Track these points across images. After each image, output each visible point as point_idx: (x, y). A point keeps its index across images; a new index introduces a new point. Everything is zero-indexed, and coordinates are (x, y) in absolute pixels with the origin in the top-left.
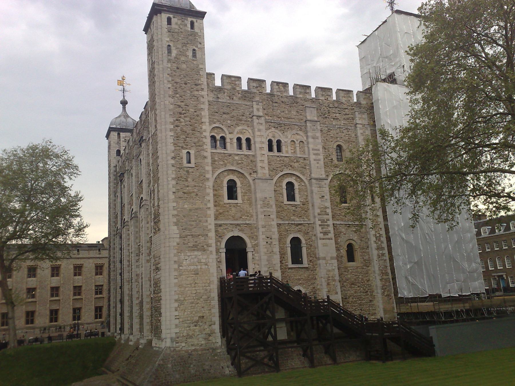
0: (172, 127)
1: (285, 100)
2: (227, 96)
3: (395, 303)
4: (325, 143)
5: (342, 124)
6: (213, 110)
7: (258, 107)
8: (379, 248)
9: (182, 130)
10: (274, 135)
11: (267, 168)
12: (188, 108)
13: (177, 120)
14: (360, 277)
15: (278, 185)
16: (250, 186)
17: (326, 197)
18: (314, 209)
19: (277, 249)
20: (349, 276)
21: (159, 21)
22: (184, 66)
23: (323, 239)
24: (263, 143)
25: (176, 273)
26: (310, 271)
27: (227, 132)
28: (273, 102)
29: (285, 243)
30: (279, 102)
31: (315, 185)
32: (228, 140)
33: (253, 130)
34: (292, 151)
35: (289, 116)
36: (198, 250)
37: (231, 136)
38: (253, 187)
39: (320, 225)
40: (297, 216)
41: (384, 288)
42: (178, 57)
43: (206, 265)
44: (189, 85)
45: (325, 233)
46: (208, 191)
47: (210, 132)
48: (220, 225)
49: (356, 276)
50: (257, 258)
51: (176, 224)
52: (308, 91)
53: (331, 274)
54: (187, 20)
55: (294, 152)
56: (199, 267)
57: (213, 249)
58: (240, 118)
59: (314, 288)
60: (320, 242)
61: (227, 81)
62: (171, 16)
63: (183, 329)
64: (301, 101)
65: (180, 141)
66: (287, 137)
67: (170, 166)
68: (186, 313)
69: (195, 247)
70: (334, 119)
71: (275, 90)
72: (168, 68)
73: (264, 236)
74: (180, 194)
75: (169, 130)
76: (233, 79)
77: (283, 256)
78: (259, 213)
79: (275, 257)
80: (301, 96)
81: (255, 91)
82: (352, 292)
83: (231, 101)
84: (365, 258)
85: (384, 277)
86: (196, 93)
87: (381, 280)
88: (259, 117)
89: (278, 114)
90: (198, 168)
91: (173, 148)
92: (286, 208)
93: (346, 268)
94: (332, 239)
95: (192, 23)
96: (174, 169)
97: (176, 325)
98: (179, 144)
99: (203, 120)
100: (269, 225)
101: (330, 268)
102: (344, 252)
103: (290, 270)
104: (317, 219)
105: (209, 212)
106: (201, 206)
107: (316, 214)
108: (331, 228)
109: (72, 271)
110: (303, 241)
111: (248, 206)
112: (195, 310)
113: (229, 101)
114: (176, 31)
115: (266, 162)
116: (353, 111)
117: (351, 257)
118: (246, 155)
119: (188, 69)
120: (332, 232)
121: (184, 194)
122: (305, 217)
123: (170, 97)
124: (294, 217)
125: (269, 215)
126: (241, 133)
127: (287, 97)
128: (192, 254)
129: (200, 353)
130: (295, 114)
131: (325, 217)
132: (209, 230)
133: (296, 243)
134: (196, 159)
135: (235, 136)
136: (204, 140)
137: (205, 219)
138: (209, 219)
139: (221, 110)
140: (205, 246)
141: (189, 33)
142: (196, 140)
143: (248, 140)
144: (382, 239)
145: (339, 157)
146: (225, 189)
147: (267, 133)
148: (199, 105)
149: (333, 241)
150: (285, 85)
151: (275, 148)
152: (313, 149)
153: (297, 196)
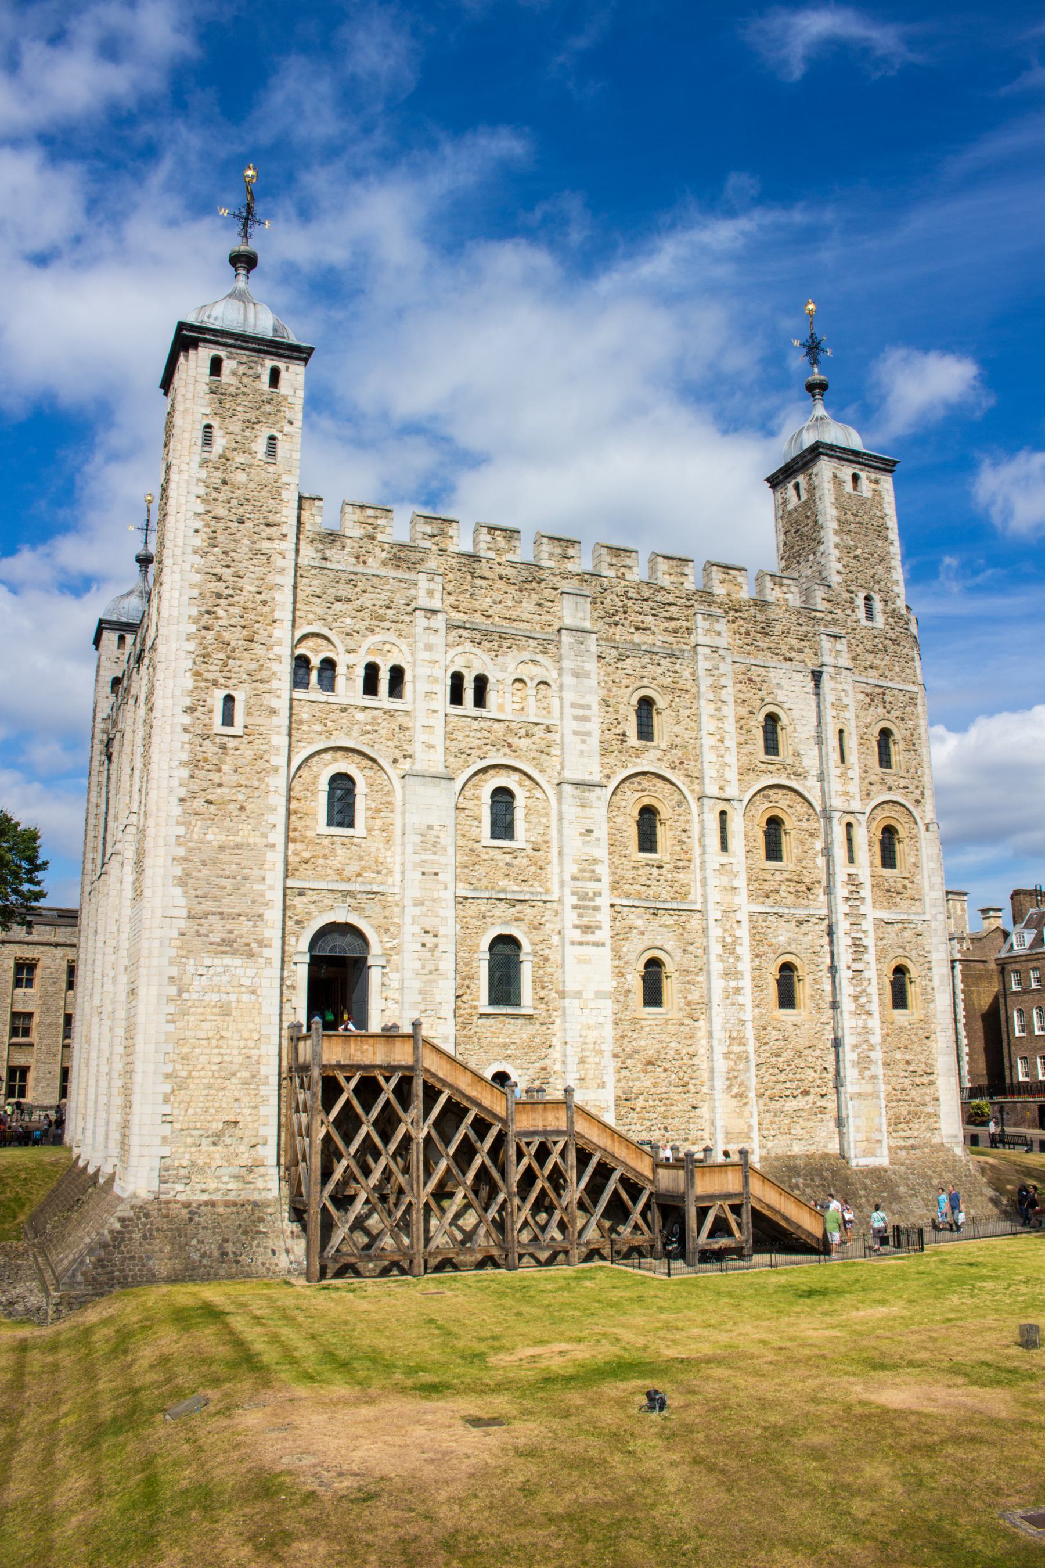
0: (193, 628)
1: (509, 572)
2: (350, 554)
3: (755, 1114)
4: (609, 690)
5: (659, 643)
6: (309, 591)
7: (432, 586)
8: (730, 974)
10: (469, 661)
11: (440, 749)
13: (208, 612)
14: (673, 1045)
15: (468, 793)
17: (596, 834)
18: (561, 864)
19: (447, 964)
20: (643, 1043)
22: (240, 477)
23: (581, 944)
24: (436, 680)
25: (171, 1009)
26: (537, 1026)
29: (474, 950)
32: (341, 669)
34: (517, 706)
35: (513, 614)
37: (351, 659)
39: (575, 907)
41: (732, 1078)
42: (228, 454)
43: (254, 992)
44: (249, 524)
45: (587, 929)
47: (294, 647)
49: (660, 1042)
50: (395, 984)
51: (181, 882)
52: (571, 552)
53: (592, 1036)
54: (262, 365)
55: (522, 709)
56: (233, 997)
57: (274, 953)
58: (381, 611)
59: (544, 1069)
60: (570, 950)
61: (355, 517)
62: (222, 353)
63: (182, 1150)
64: (551, 577)
65: (211, 668)
66: (504, 670)
67: (179, 729)
68: (191, 1111)
69: (227, 946)
72: (199, 480)
73: (417, 929)
74: (198, 804)
75: (184, 636)
76: (370, 512)
77: (466, 983)
78: (409, 866)
79: (442, 983)
81: (428, 544)
82: (648, 1083)
83: (360, 569)
84: (690, 998)
85: (736, 1049)
87: (727, 1055)
89: (485, 606)
91: (189, 682)
92: (486, 857)
93: (635, 1021)
94: (603, 945)
95: (275, 374)
96: (187, 737)
97: (164, 1138)
98: (206, 675)
99: (277, 615)
100: (434, 901)
101: (591, 1022)
102: (635, 982)
103: (482, 1021)
104: (567, 891)
106: (251, 841)
107: (567, 878)
108: (604, 917)
109: (11, 974)
110: (526, 947)
111: (381, 846)
112: (217, 1105)
113: (352, 569)
114: (232, 390)
115: (440, 731)
116: (690, 612)
117: (653, 995)
119: (252, 485)
120: (606, 923)
122: (536, 884)
123: (196, 553)
125: (436, 874)
127: (513, 564)
128: (217, 961)
129: (221, 1210)
131: (591, 886)
133: (505, 952)
136: (275, 666)
137: (261, 872)
138: (269, 875)
139: (331, 591)
140: (254, 945)
141: (264, 398)
143: (397, 674)
144: (739, 950)
145: (645, 729)
147: (450, 655)
148: (270, 577)
149: (606, 952)
150: (511, 534)
151: (469, 695)
152: (573, 705)
153: (520, 826)
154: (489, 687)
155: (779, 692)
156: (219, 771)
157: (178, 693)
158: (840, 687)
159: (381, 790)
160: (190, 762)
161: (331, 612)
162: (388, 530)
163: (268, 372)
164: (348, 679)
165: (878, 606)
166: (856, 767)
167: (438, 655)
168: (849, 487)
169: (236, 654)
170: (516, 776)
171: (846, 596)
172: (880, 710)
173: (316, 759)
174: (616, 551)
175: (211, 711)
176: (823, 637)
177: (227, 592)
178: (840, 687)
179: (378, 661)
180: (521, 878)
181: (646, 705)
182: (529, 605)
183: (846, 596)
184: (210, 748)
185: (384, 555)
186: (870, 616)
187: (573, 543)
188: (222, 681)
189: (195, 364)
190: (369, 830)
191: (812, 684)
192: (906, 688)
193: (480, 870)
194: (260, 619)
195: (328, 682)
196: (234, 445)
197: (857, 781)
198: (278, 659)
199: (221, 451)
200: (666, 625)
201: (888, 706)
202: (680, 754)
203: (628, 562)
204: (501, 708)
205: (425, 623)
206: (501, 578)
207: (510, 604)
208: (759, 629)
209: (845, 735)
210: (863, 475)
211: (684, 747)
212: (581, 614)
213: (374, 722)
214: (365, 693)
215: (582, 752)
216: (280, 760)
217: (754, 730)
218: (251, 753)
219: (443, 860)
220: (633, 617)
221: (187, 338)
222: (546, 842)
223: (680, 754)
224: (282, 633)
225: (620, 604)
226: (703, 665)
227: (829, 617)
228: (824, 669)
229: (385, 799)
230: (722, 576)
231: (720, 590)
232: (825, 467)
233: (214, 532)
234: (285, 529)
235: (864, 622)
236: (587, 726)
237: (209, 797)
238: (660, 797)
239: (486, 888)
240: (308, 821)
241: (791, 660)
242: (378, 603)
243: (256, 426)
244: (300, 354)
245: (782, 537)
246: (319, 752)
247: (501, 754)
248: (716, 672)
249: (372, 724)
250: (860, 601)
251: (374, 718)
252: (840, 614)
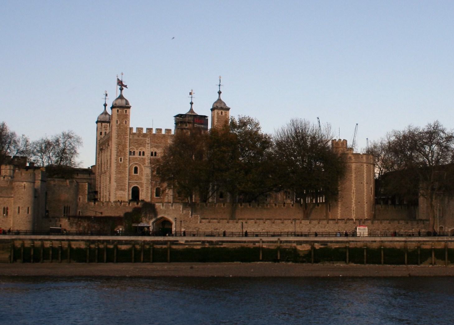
0: (116, 149)
1: (160, 136)
19: (150, 192)
27: (136, 149)
32: (136, 153)
33: (146, 149)
36: (122, 190)
37: (137, 151)
48: (131, 182)
51: (115, 182)
57: (127, 190)
69: (121, 190)
81: (148, 133)
88: (148, 144)
91: (116, 156)
95: (126, 111)
118: (142, 158)
121: (119, 172)
127: (161, 135)
132: (126, 184)
134: (124, 160)
135: (138, 151)
143: (144, 153)
150: (161, 130)
167: (149, 150)
168: (220, 114)
190: (140, 174)
195: (134, 154)
198: (127, 152)
210: (223, 111)
213: (140, 159)
216: (128, 166)
224: (128, 149)
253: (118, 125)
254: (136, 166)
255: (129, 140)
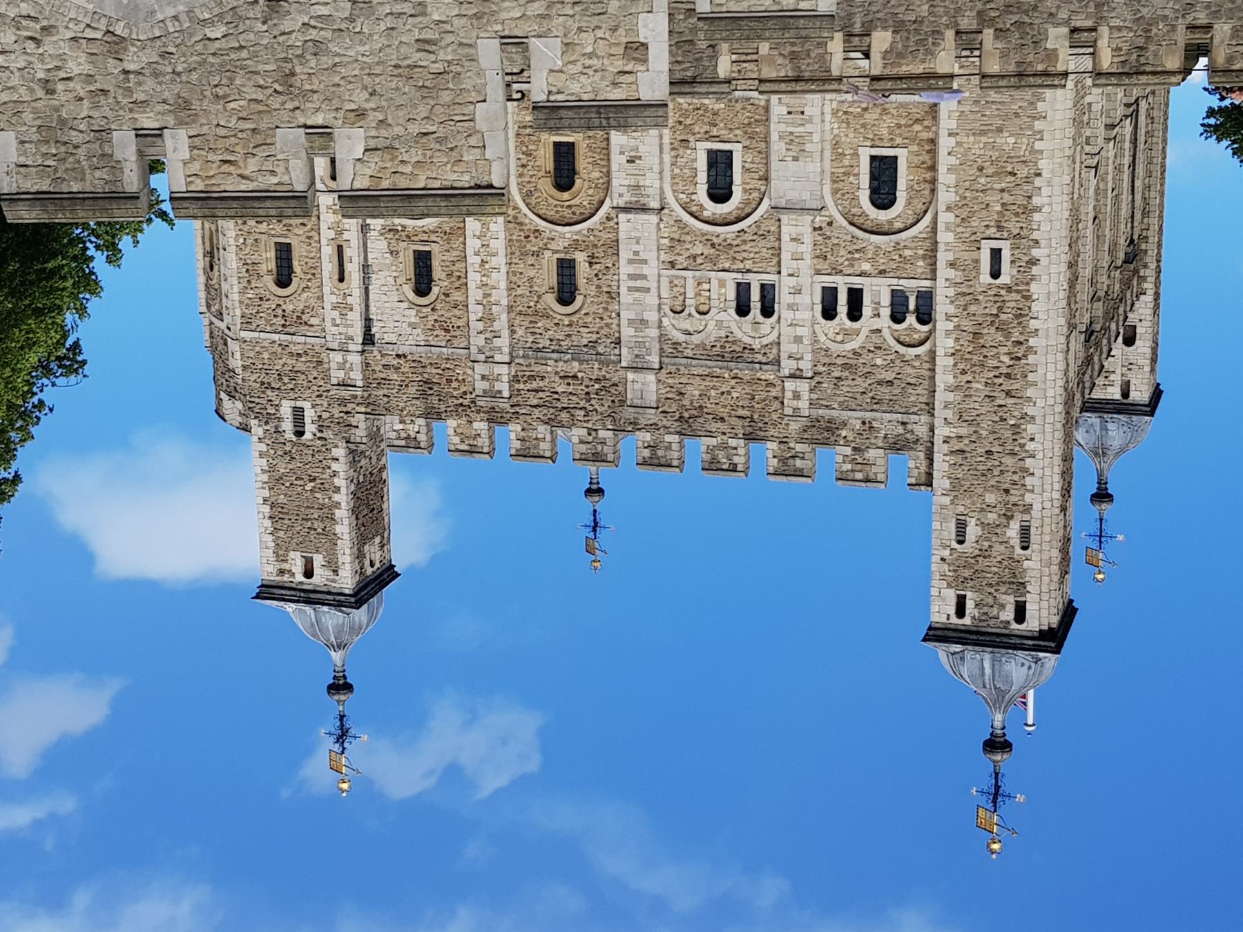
0: (1032, 342)
1: (714, 426)
4: (606, 309)
5: (550, 362)
6: (920, 390)
9: (1008, 335)
10: (755, 330)
11: (785, 238)
12: (987, 390)
13: (1019, 359)
15: (755, 195)
16: (835, 192)
17: (623, 159)
21: (1044, 613)
22: (991, 498)
24: (791, 307)
27: (886, 333)
28: (752, 417)
30: (734, 421)
31: (649, 191)
32: (886, 312)
38: (827, 189)
40: (706, 111)
44: (981, 450)
46: (951, 179)
47: (931, 332)
54: (973, 618)
55: (699, 284)
58: (847, 373)
61: (874, 469)
62: (1014, 626)
65: (1014, 304)
66: (719, 324)
70: (575, 377)
71: (741, 451)
74: (1023, 172)
75: (1040, 333)
76: (859, 476)
78: (817, 120)
80: (668, 438)
81: (799, 448)
86: (963, 431)
90: (973, 238)
91: (1034, 287)
92: (737, 132)
95: (961, 612)
96: (1035, 235)
98: (1018, 297)
99: (951, 361)
105: (953, 125)
106: (971, 139)
113: (878, 415)
114: (1003, 589)
115: (785, 256)
119: (980, 491)
122: (685, 106)
123: (1033, 418)
124: (717, 107)
126: (847, 333)
127: (710, 434)
130: (689, 388)
134: (977, 261)
135: (867, 320)
136: (951, 310)
141: (971, 583)
142: (972, 308)
143: (829, 312)
146: (902, 184)
148: (959, 398)
150: (712, 466)
151: (755, 295)
154: (734, 304)
155: (413, 320)
156: (1003, 205)
157: (1045, 278)
158: (342, 329)
159: (843, 195)
160: (1032, 211)
161: (896, 369)
162: (840, 459)
163: (967, 612)
164: (879, 303)
165: (288, 426)
166: (324, 242)
167: (787, 331)
168: (318, 560)
169: (990, 319)
170: (706, 214)
171: (328, 434)
172: (289, 307)
173: (909, 222)
174: (597, 458)
175: (1012, 262)
176: (360, 383)
177: (1000, 381)
178: (342, 329)
179: (848, 324)
180: (701, 112)
181: (566, 294)
182: (693, 392)
183: (328, 434)
184: (1013, 226)
185: (844, 433)
186: (298, 414)
187: (644, 463)
188: (1003, 292)
189: (1041, 616)
191: (374, 330)
192: (256, 334)
193: (743, 117)
194: (968, 356)
196: (998, 531)
197: (323, 226)
198: (948, 317)
199: (1012, 522)
200: (541, 384)
201: (280, 312)
202: (528, 247)
203: (583, 448)
204: (722, 284)
205: (802, 365)
206: (722, 419)
207: (713, 393)
208: (436, 388)
209: (337, 277)
210: (299, 577)
211: (524, 254)
212: (637, 386)
214: (861, 290)
215: (638, 243)
216: (945, 218)
217: (443, 276)
218: (974, 224)
219: (782, 127)
220: (581, 389)
221: (1053, 639)
222: (673, 149)
223: (528, 247)
224: (944, 343)
225: (593, 402)
226: (504, 342)
227: (350, 407)
228: (360, 348)
229: (840, 185)
230: (479, 442)
231: (480, 426)
232: (347, 581)
233: (1015, 440)
234: (946, 448)
235: (306, 405)
236: (631, 270)
237: (1013, 179)
238: (551, 200)
239: (737, 101)
240: (916, 160)
241: (398, 356)
242: (849, 382)
243: (977, 552)
244: (938, 634)
245: (385, 506)
246: (906, 229)
247: (722, 237)
248: (488, 335)
249: (853, 259)
250: (310, 428)
251: (852, 266)
252: (336, 411)
253: (1018, 516)
254: (882, 216)
255: (938, 405)
